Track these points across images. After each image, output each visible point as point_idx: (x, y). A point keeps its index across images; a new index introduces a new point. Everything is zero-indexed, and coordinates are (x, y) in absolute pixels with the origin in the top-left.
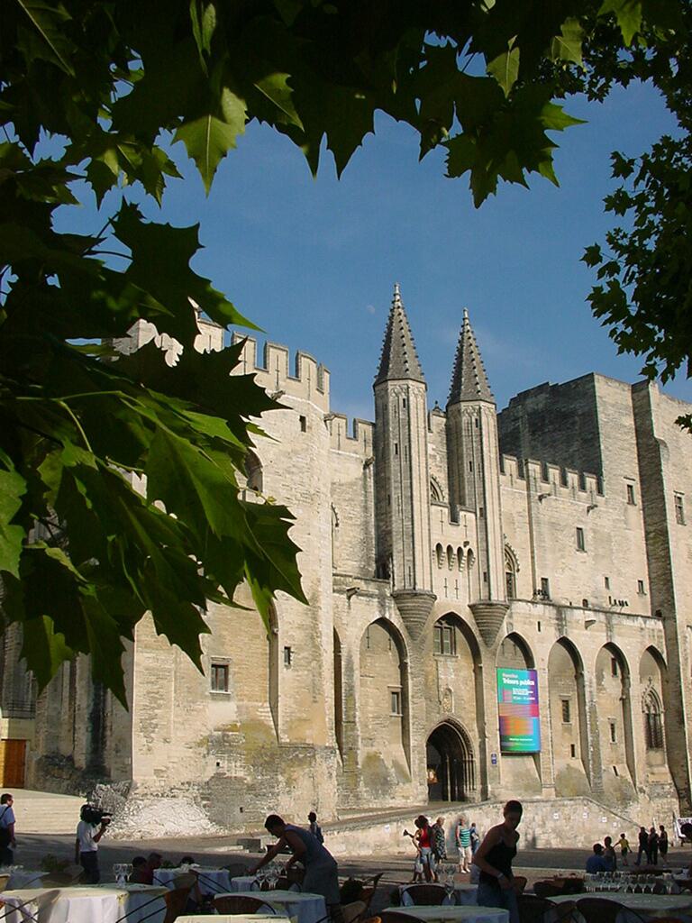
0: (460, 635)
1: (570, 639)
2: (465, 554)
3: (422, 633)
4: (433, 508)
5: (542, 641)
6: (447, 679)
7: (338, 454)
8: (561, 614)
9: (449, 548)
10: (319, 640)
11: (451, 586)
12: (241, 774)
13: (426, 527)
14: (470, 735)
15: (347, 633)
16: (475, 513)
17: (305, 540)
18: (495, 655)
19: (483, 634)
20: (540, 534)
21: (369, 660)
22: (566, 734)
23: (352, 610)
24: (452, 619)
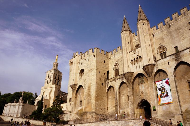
0: (144, 77)
1: (183, 61)
3: (131, 81)
4: (130, 53)
5: (170, 67)
6: (142, 89)
9: (135, 59)
11: (138, 68)
13: (126, 59)
14: (150, 102)
16: (140, 47)
18: (152, 78)
19: (148, 74)
20: (172, 35)
21: (123, 91)
24: (140, 75)
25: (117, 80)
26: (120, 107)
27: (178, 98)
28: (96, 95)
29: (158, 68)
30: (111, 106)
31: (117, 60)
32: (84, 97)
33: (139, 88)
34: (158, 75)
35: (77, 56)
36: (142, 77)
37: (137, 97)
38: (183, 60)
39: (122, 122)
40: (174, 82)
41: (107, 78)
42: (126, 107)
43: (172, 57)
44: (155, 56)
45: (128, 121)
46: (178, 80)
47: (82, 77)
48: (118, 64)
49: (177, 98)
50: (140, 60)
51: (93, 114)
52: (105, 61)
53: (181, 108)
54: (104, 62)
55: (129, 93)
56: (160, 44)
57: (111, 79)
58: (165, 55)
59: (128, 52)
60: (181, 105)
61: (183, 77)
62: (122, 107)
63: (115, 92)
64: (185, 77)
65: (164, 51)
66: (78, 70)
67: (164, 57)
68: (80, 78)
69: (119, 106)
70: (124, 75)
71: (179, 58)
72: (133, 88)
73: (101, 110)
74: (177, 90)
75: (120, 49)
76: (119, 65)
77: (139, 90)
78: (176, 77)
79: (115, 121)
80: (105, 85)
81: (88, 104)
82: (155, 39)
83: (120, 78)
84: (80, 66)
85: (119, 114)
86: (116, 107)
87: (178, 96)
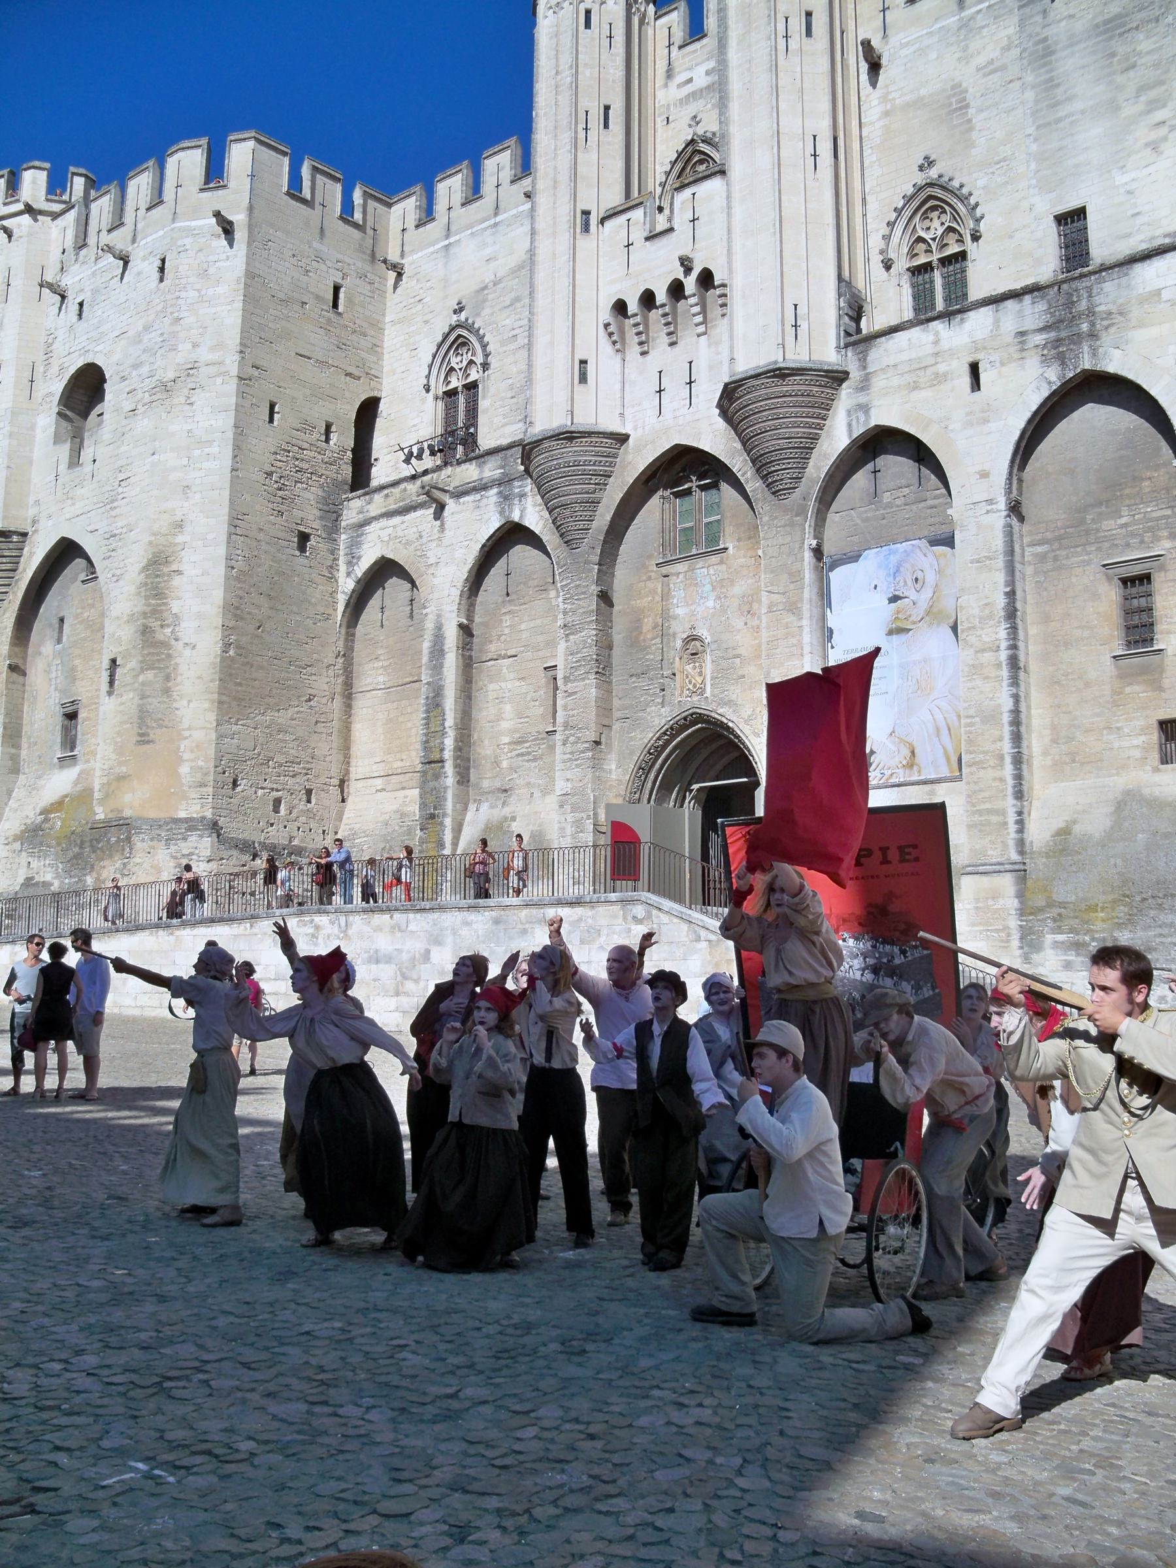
1: (1111, 369)
2: (690, 284)
4: (609, 224)
7: (496, 225)
8: (1070, 304)
9: (648, 299)
10: (168, 631)
12: (48, 877)
13: (564, 283)
15: (436, 581)
16: (723, 172)
17: (148, 467)
18: (802, 512)
21: (507, 621)
22: (1136, 690)
23: (446, 532)
25: (451, 505)
26: (463, 778)
27: (1016, 722)
28: (227, 646)
29: (873, 412)
30: (380, 769)
31: (464, 289)
32: (106, 664)
33: (666, 596)
34: (860, 480)
35: (29, 210)
36: (703, 488)
37: (642, 683)
38: (1114, 363)
39: (467, 923)
40: (1000, 562)
41: (347, 471)
42: (521, 782)
43: (1020, 315)
44: (860, 283)
45: (524, 912)
46: (1040, 549)
47: (87, 454)
48: (481, 338)
49: (1006, 718)
50: (704, 311)
51: (193, 838)
52: (337, 289)
53: (1020, 813)
54: (330, 296)
55: (562, 646)
56: (929, 162)
57: (396, 491)
58: (957, 288)
59: (586, 213)
60: (1031, 788)
61: (1082, 521)
62: (486, 784)
63: (430, 625)
64: (1108, 524)
65: (954, 249)
66: (40, 369)
67: (940, 305)
68: (63, 467)
69: (456, 766)
70: (528, 450)
71: (1076, 339)
72: (605, 597)
73: (277, 802)
74: (1014, 647)
75: (506, 175)
76: (484, 346)
77: (666, 615)
78: (1022, 519)
79: (397, 915)
80: (323, 546)
81: (144, 739)
82: (884, 99)
83: (481, 487)
84: (61, 334)
85: (455, 844)
86: (424, 773)
87: (1016, 698)
